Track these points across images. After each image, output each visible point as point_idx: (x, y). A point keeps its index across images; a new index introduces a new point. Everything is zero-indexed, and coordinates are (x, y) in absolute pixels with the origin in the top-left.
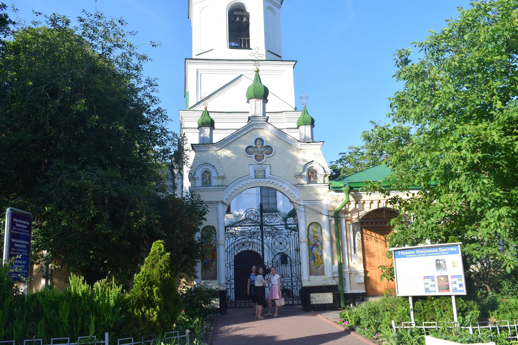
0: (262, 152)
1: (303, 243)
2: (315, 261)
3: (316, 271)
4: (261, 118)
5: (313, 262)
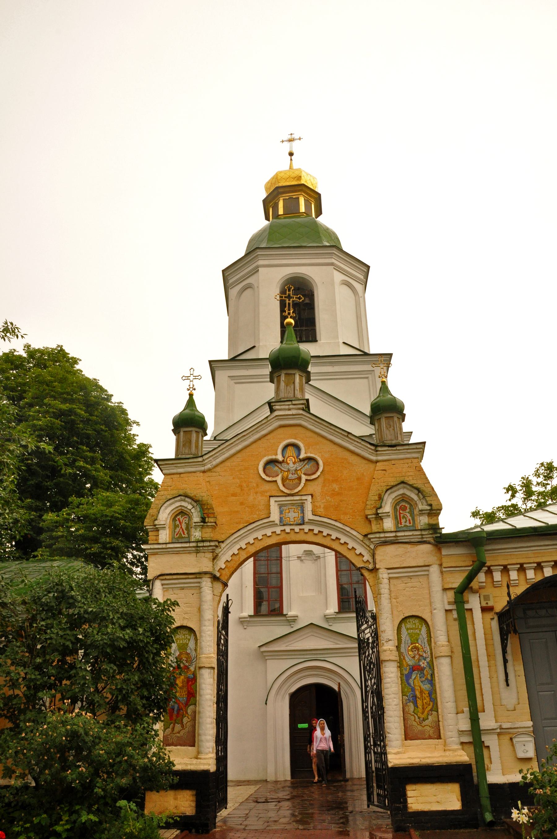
0: (296, 470)
1: (387, 664)
2: (416, 705)
3: (420, 728)
4: (294, 402)
5: (411, 707)
